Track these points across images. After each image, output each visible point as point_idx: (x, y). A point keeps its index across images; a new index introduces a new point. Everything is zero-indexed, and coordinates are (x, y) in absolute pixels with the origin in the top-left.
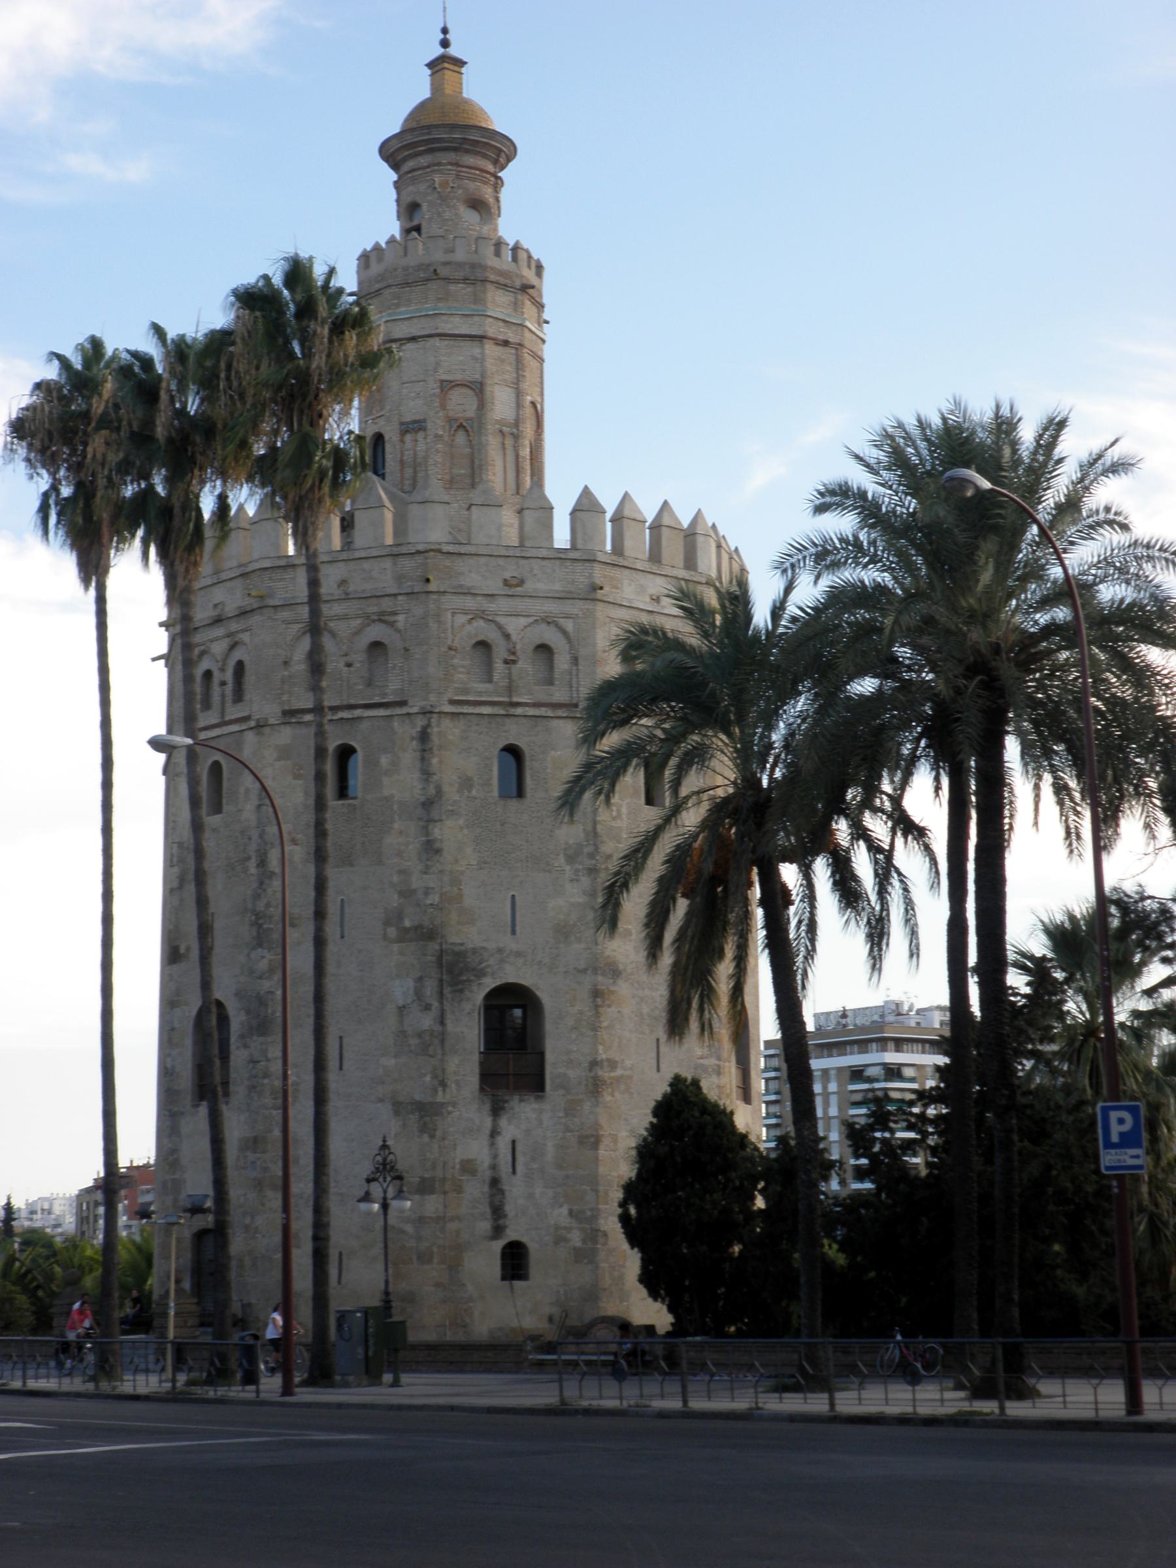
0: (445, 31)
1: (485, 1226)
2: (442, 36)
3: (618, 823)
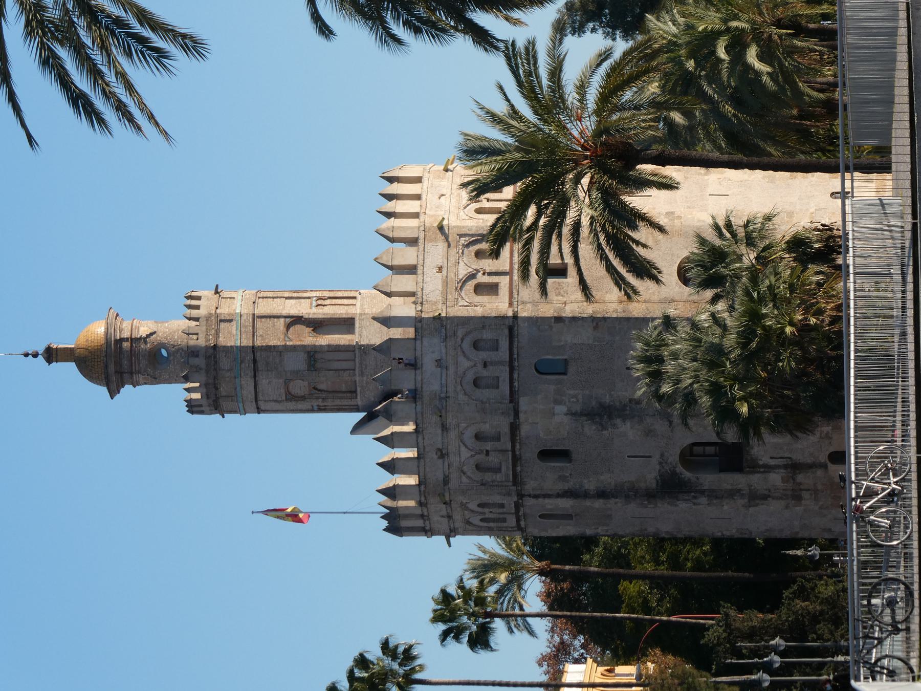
0: (26, 355)
1: (819, 473)
2: (30, 356)
3: (580, 397)
